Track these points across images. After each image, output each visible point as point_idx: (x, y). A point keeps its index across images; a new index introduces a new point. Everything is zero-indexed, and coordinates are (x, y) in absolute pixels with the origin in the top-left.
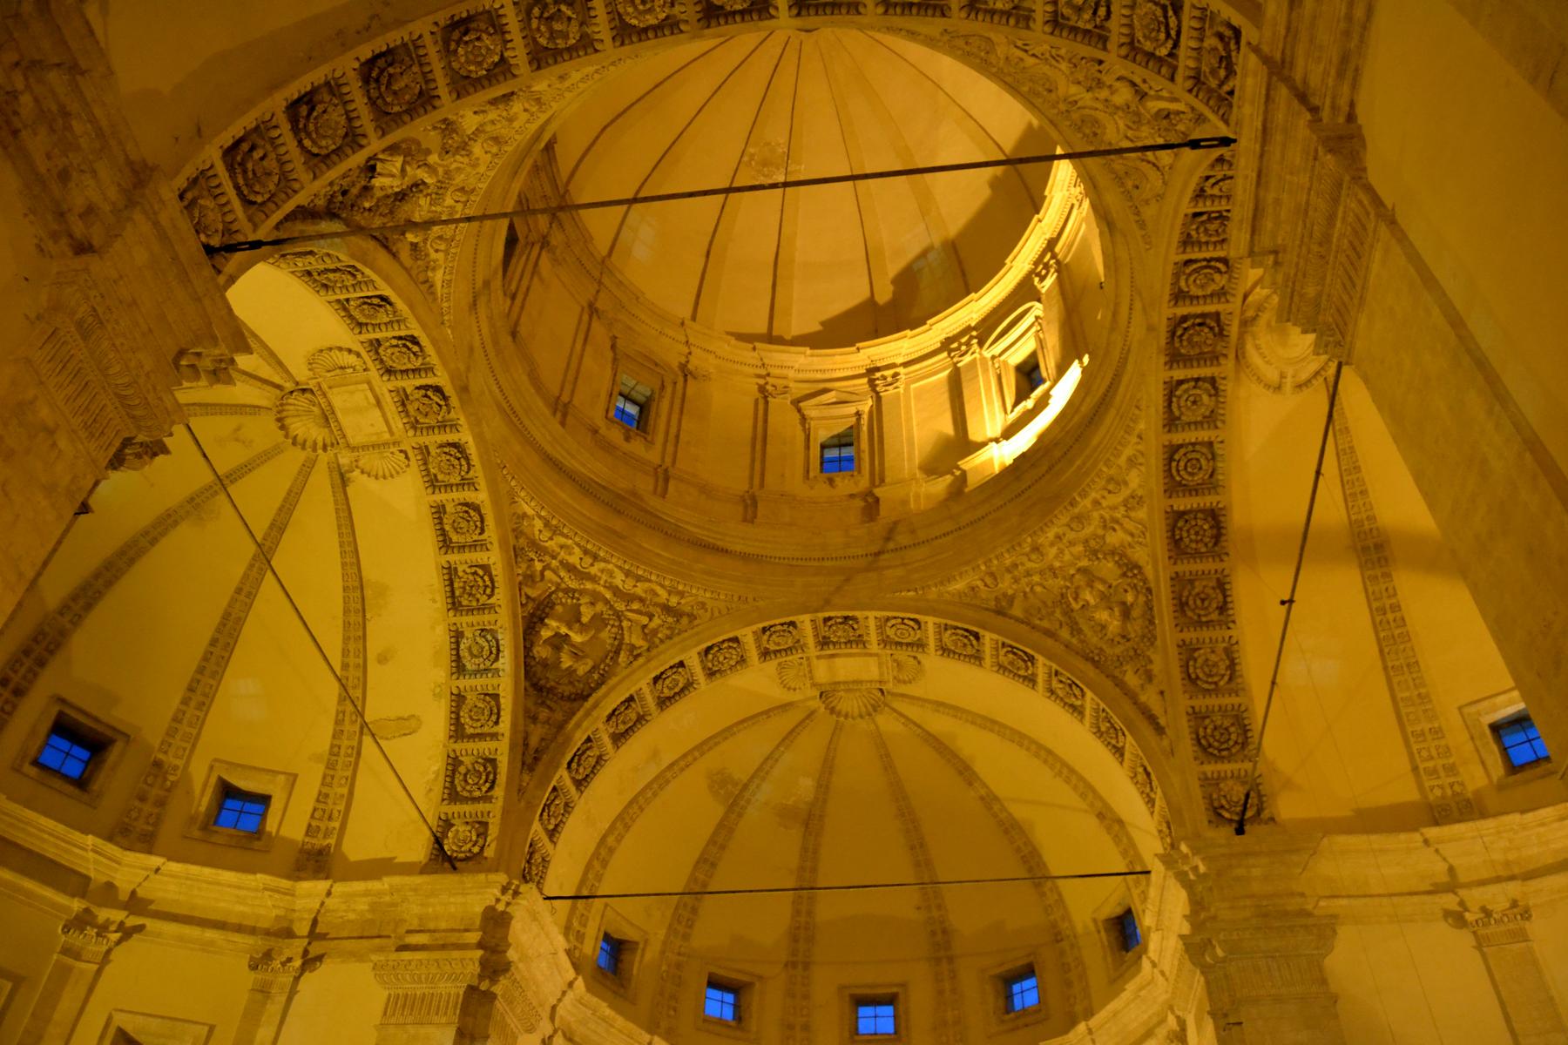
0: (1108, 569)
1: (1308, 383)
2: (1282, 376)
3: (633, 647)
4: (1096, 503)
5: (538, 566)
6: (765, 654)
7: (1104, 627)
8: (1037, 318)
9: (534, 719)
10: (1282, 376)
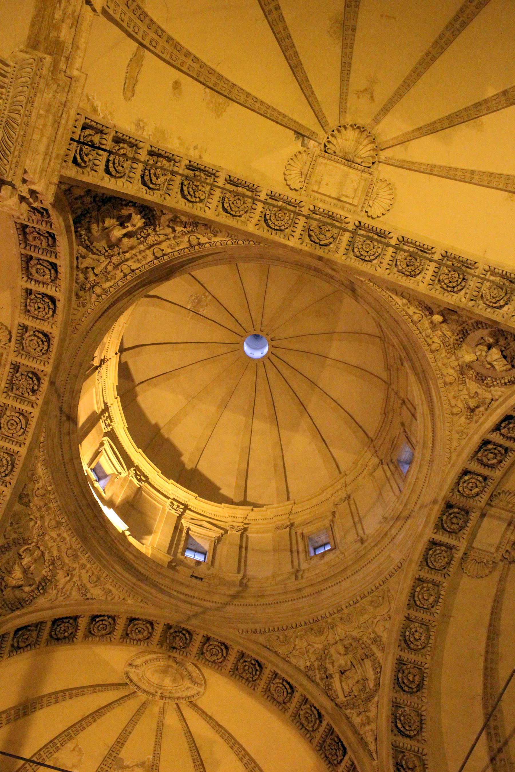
1: (128, 677)
4: (83, 566)
5: (179, 229)
7: (10, 572)
8: (120, 473)
10: (136, 666)
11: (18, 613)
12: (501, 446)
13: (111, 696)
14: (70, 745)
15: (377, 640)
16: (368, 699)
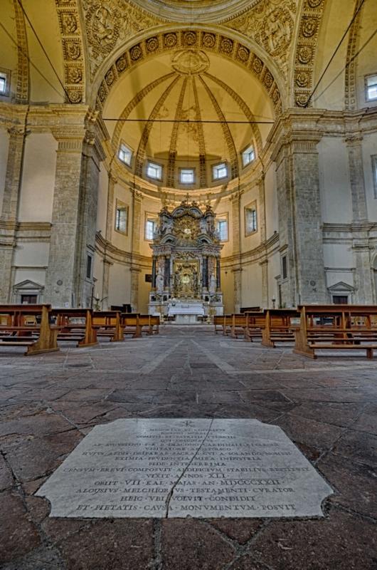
1: (174, 68)
10: (176, 61)
11: (112, 52)
13: (170, 80)
14: (162, 108)
16: (286, 47)
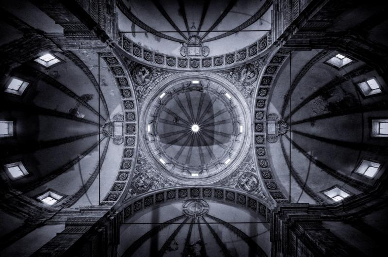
0: (148, 182)
2: (186, 207)
3: (137, 87)
5: (159, 73)
6: (127, 113)
9: (131, 63)
10: (186, 207)
12: (262, 100)
14: (173, 242)
15: (253, 170)
